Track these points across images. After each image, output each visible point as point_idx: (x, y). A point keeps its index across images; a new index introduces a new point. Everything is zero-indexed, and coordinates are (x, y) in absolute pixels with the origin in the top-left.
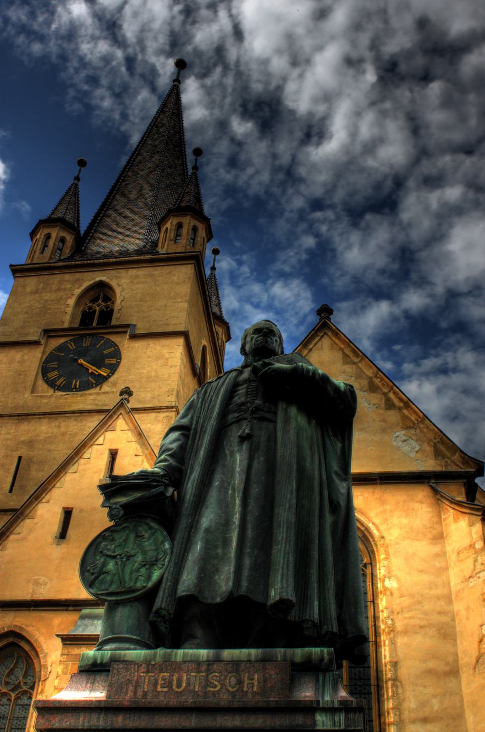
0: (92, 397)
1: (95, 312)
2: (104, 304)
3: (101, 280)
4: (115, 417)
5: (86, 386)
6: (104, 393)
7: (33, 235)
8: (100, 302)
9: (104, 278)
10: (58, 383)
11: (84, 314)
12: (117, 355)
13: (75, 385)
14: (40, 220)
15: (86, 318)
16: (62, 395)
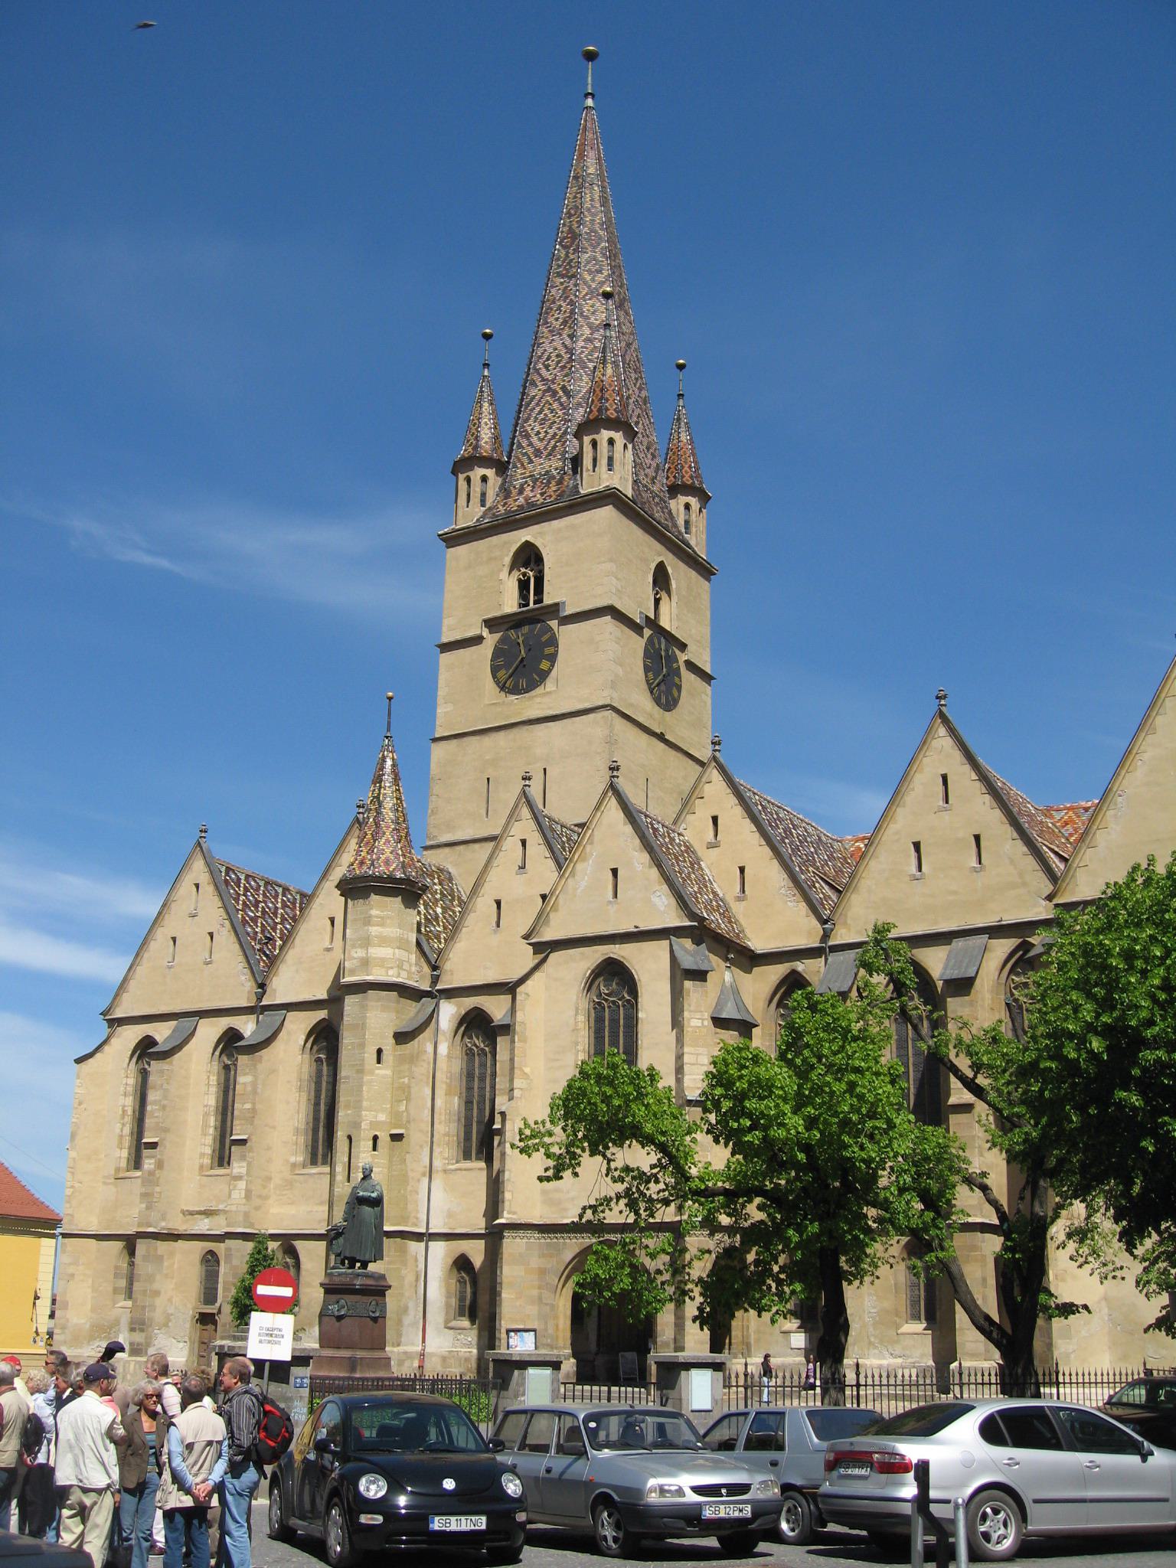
0: (538, 700)
1: (529, 578)
2: (536, 568)
3: (527, 542)
4: (520, 805)
5: (532, 686)
6: (548, 693)
7: (455, 472)
8: (532, 565)
9: (529, 538)
10: (507, 685)
11: (520, 581)
12: (553, 642)
13: (523, 685)
14: (455, 463)
15: (523, 585)
16: (512, 701)
